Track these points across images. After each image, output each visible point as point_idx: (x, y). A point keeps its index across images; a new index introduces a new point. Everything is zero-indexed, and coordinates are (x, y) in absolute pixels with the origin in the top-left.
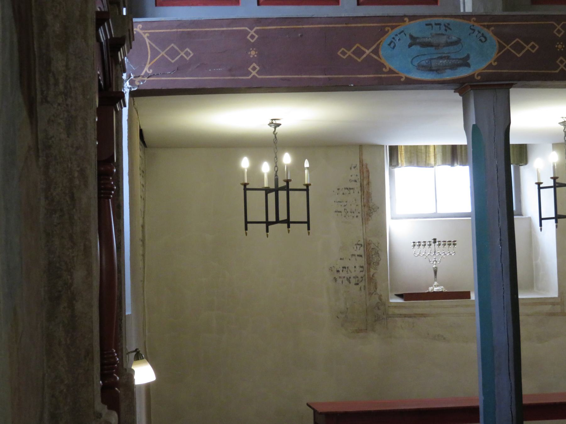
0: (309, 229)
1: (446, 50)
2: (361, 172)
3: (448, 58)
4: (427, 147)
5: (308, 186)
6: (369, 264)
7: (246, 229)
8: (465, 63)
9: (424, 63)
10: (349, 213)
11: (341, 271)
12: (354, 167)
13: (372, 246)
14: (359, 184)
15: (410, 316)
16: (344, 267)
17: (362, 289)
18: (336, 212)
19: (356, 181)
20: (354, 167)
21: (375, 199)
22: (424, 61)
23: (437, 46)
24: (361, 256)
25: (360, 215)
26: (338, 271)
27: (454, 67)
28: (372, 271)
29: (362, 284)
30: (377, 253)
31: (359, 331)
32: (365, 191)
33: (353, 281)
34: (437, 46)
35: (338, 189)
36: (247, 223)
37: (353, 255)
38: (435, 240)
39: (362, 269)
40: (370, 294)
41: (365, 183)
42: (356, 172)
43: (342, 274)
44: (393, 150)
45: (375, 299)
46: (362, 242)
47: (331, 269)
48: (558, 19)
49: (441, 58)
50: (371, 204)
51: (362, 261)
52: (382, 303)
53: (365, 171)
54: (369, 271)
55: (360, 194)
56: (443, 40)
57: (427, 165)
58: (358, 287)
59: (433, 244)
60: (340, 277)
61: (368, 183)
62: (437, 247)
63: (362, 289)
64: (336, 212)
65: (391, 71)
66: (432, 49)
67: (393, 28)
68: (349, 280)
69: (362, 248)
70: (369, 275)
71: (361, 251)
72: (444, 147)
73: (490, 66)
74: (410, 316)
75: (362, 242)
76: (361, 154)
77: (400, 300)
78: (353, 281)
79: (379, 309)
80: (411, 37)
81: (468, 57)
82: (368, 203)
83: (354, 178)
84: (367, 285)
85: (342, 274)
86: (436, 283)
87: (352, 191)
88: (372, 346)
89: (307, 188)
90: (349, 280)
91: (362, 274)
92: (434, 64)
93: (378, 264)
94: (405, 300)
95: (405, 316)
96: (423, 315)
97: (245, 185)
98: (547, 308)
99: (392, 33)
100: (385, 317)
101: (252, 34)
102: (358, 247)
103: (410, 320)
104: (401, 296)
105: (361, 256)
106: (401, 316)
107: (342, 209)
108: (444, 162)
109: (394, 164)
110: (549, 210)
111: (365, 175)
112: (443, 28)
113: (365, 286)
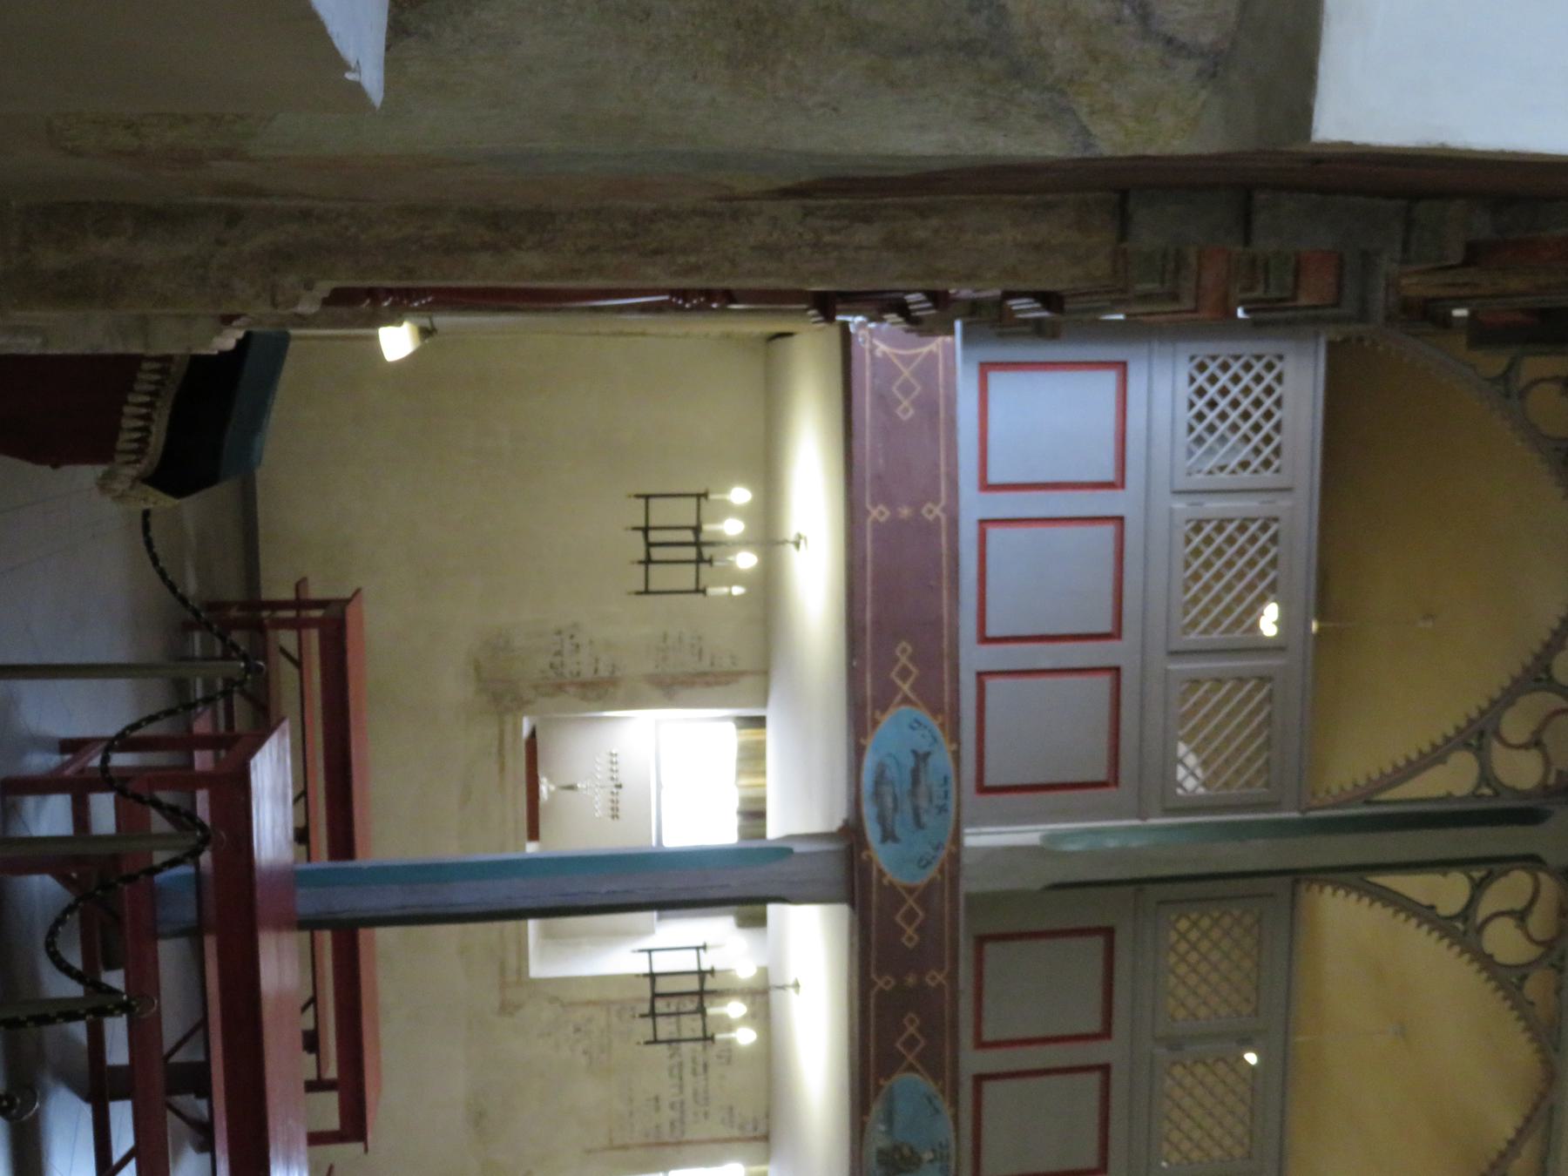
1: (907, 807)
3: (895, 809)
4: (763, 773)
5: (704, 592)
7: (638, 496)
8: (888, 836)
9: (888, 773)
22: (892, 772)
23: (913, 793)
27: (881, 819)
28: (572, 690)
29: (551, 674)
30: (599, 697)
31: (478, 668)
33: (557, 660)
34: (913, 793)
36: (647, 497)
37: (597, 660)
38: (619, 786)
40: (536, 687)
42: (726, 664)
44: (760, 722)
46: (618, 674)
47: (575, 625)
48: (953, 977)
49: (895, 799)
51: (587, 674)
52: (521, 705)
54: (572, 684)
56: (923, 803)
57: (740, 773)
61: (708, 684)
65: (875, 723)
66: (907, 786)
67: (942, 726)
68: (558, 653)
71: (604, 672)
72: (763, 800)
73: (881, 873)
75: (618, 674)
76: (753, 673)
77: (526, 732)
78: (557, 660)
80: (927, 755)
81: (895, 839)
82: (677, 682)
86: (553, 788)
92: (887, 789)
96: (502, 769)
97: (705, 495)
98: (512, 962)
99: (933, 724)
101: (934, 511)
104: (533, 734)
108: (744, 800)
110: (663, 963)
112: (940, 802)
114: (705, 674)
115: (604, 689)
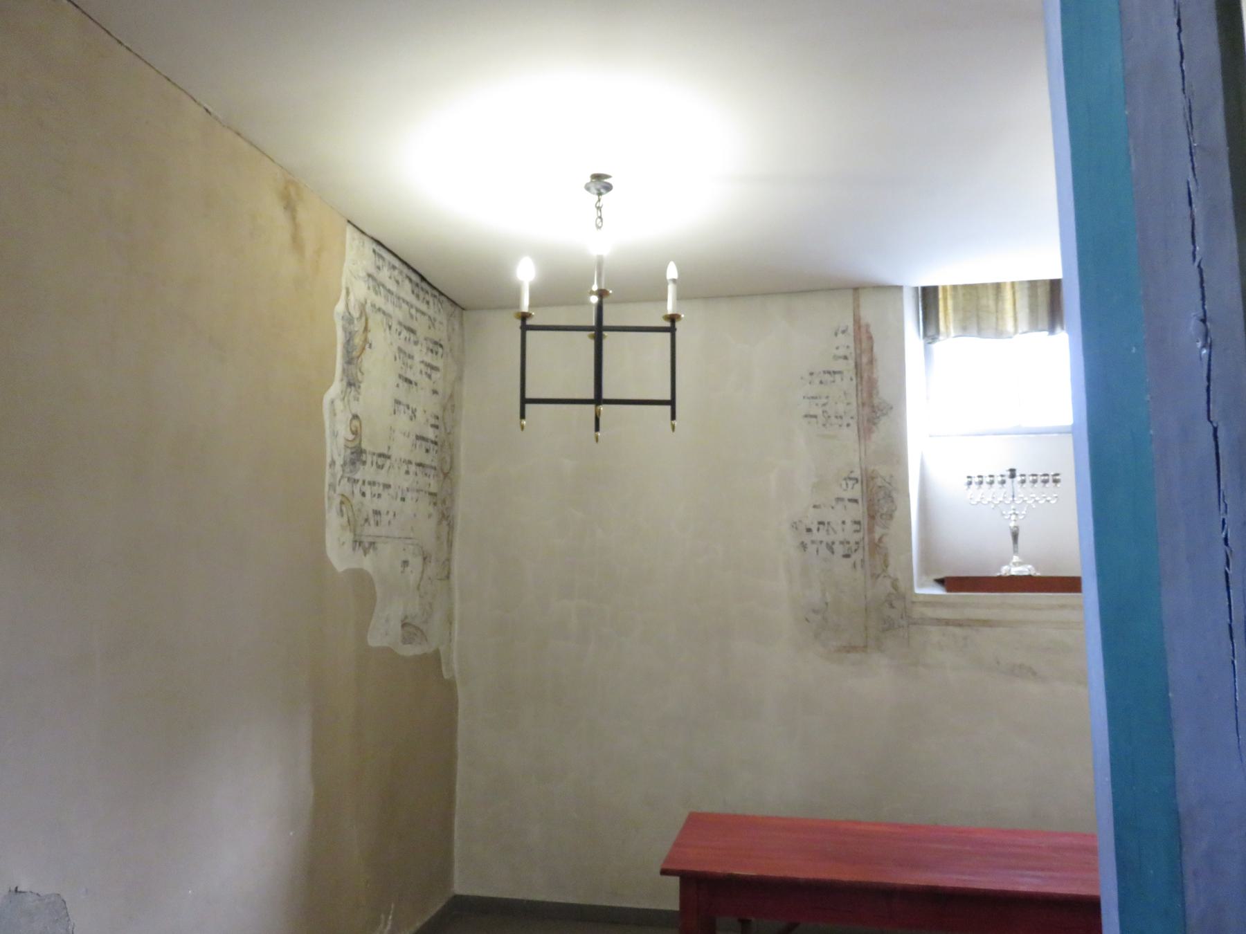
0: (673, 417)
2: (857, 339)
4: (998, 287)
5: (673, 319)
6: (872, 517)
7: (523, 416)
10: (833, 420)
11: (815, 531)
12: (844, 332)
13: (879, 482)
14: (851, 363)
15: (958, 624)
16: (821, 523)
17: (859, 566)
18: (806, 416)
19: (846, 358)
20: (844, 332)
21: (884, 392)
24: (856, 501)
25: (853, 423)
26: (809, 530)
28: (878, 532)
29: (857, 557)
30: (889, 497)
31: (851, 649)
32: (865, 375)
33: (839, 549)
35: (811, 374)
36: (524, 401)
37: (839, 499)
38: (1013, 473)
39: (857, 527)
40: (875, 576)
41: (865, 360)
43: (816, 536)
44: (928, 297)
45: (884, 586)
46: (857, 474)
47: (795, 526)
50: (876, 401)
51: (858, 512)
52: (899, 596)
53: (864, 337)
54: (871, 530)
55: (854, 382)
57: (999, 333)
58: (850, 561)
59: (1009, 480)
60: (813, 542)
61: (871, 361)
62: (1018, 487)
63: (859, 566)
64: (806, 416)
68: (830, 547)
69: (858, 486)
70: (871, 541)
71: (856, 491)
72: (1033, 285)
74: (958, 624)
75: (857, 474)
76: (856, 307)
77: (939, 591)
78: (839, 549)
79: (892, 606)
82: (866, 398)
83: (841, 352)
84: (867, 558)
85: (816, 536)
86: (1016, 559)
87: (838, 377)
88: (875, 681)
89: (671, 325)
90: (830, 547)
91: (858, 537)
93: (891, 517)
94: (949, 590)
95: (947, 623)
96: (986, 623)
97: (524, 317)
100: (904, 622)
102: (850, 483)
103: (957, 631)
104: (941, 582)
105: (856, 501)
106: (939, 622)
107: (818, 411)
108: (1034, 326)
109: (931, 332)
111: (865, 345)
113: (863, 561)
114: (857, 366)
115: (878, 494)
